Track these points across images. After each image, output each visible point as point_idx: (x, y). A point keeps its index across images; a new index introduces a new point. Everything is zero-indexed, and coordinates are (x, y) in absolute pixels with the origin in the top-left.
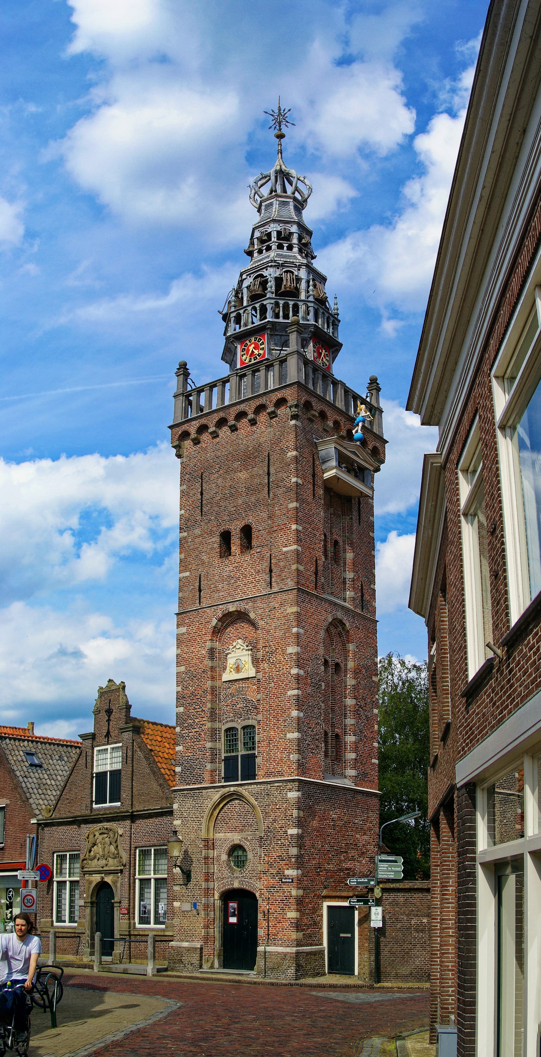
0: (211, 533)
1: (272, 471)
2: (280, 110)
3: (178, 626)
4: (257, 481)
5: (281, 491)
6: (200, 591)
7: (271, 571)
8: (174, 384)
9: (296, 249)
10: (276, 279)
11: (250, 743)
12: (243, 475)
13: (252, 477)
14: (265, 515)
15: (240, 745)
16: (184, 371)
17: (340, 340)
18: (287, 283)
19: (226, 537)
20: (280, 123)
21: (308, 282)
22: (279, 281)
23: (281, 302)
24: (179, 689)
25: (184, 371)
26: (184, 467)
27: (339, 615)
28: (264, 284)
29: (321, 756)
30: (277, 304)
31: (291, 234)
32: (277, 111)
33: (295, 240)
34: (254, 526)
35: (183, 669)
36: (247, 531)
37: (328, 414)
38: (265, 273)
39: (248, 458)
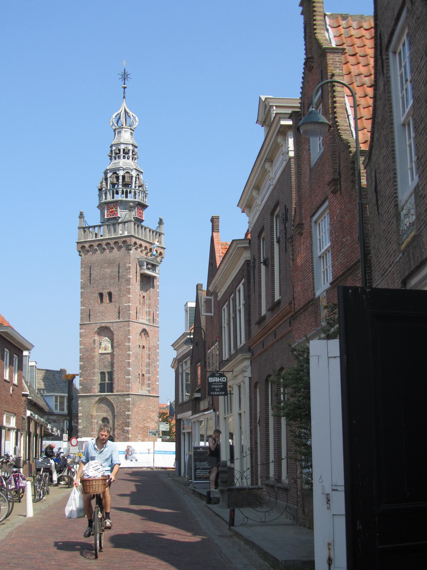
0: (94, 293)
1: (120, 271)
2: (125, 70)
3: (80, 329)
4: (114, 274)
5: (123, 280)
6: (90, 316)
7: (119, 312)
8: (77, 222)
9: (131, 158)
10: (123, 176)
11: (111, 378)
12: (108, 270)
13: (112, 272)
14: (117, 289)
15: (107, 379)
18: (127, 180)
19: (101, 295)
21: (136, 178)
22: (124, 177)
23: (125, 190)
24: (81, 355)
26: (82, 260)
27: (145, 327)
28: (117, 178)
29: (138, 383)
30: (123, 191)
31: (129, 150)
32: (123, 72)
33: (131, 154)
34: (112, 293)
35: (82, 347)
36: (110, 294)
37: (143, 244)
38: (118, 173)
39: (110, 263)
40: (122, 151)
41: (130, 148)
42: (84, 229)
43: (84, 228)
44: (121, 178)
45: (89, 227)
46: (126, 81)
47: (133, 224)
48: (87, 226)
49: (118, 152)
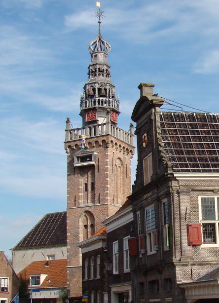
16: (68, 121)
17: (120, 111)
20: (100, 16)
22: (100, 90)
25: (68, 121)
38: (93, 85)
40: (98, 69)
41: (105, 68)
42: (70, 131)
43: (70, 131)
44: (97, 90)
45: (75, 130)
46: (101, 18)
47: (110, 125)
48: (72, 129)
49: (94, 70)
